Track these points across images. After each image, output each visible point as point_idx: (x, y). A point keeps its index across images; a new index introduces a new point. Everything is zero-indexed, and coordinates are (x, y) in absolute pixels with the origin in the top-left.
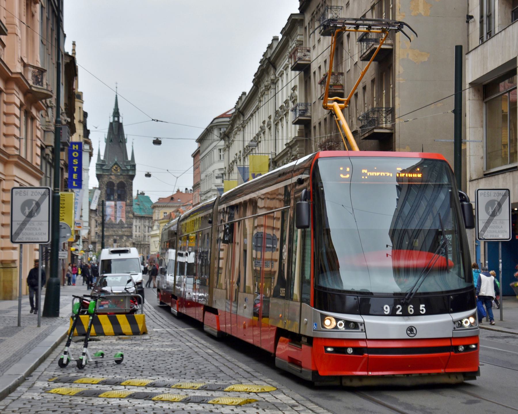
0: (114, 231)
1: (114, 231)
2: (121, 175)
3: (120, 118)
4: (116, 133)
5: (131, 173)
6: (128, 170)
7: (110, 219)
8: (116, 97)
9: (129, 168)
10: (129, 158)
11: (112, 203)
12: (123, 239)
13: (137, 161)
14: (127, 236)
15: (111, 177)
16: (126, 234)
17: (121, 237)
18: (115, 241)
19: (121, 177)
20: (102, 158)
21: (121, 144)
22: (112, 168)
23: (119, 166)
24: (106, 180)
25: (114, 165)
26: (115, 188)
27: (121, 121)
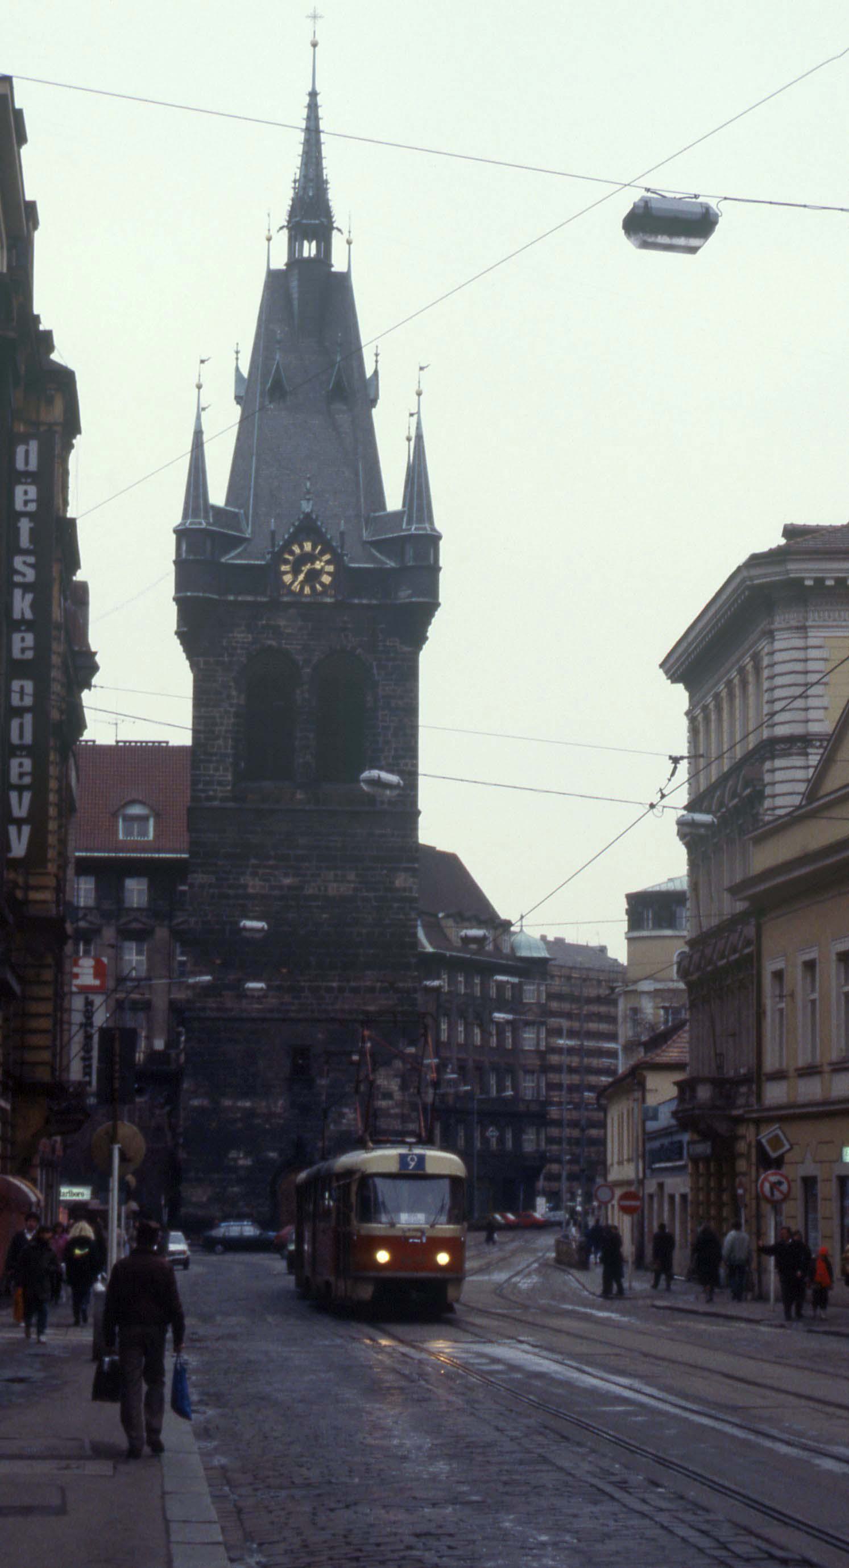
3: (337, 241)
4: (308, 342)
8: (313, 107)
13: (442, 519)
20: (217, 495)
21: (338, 406)
22: (278, 558)
25: (296, 537)
27: (338, 264)
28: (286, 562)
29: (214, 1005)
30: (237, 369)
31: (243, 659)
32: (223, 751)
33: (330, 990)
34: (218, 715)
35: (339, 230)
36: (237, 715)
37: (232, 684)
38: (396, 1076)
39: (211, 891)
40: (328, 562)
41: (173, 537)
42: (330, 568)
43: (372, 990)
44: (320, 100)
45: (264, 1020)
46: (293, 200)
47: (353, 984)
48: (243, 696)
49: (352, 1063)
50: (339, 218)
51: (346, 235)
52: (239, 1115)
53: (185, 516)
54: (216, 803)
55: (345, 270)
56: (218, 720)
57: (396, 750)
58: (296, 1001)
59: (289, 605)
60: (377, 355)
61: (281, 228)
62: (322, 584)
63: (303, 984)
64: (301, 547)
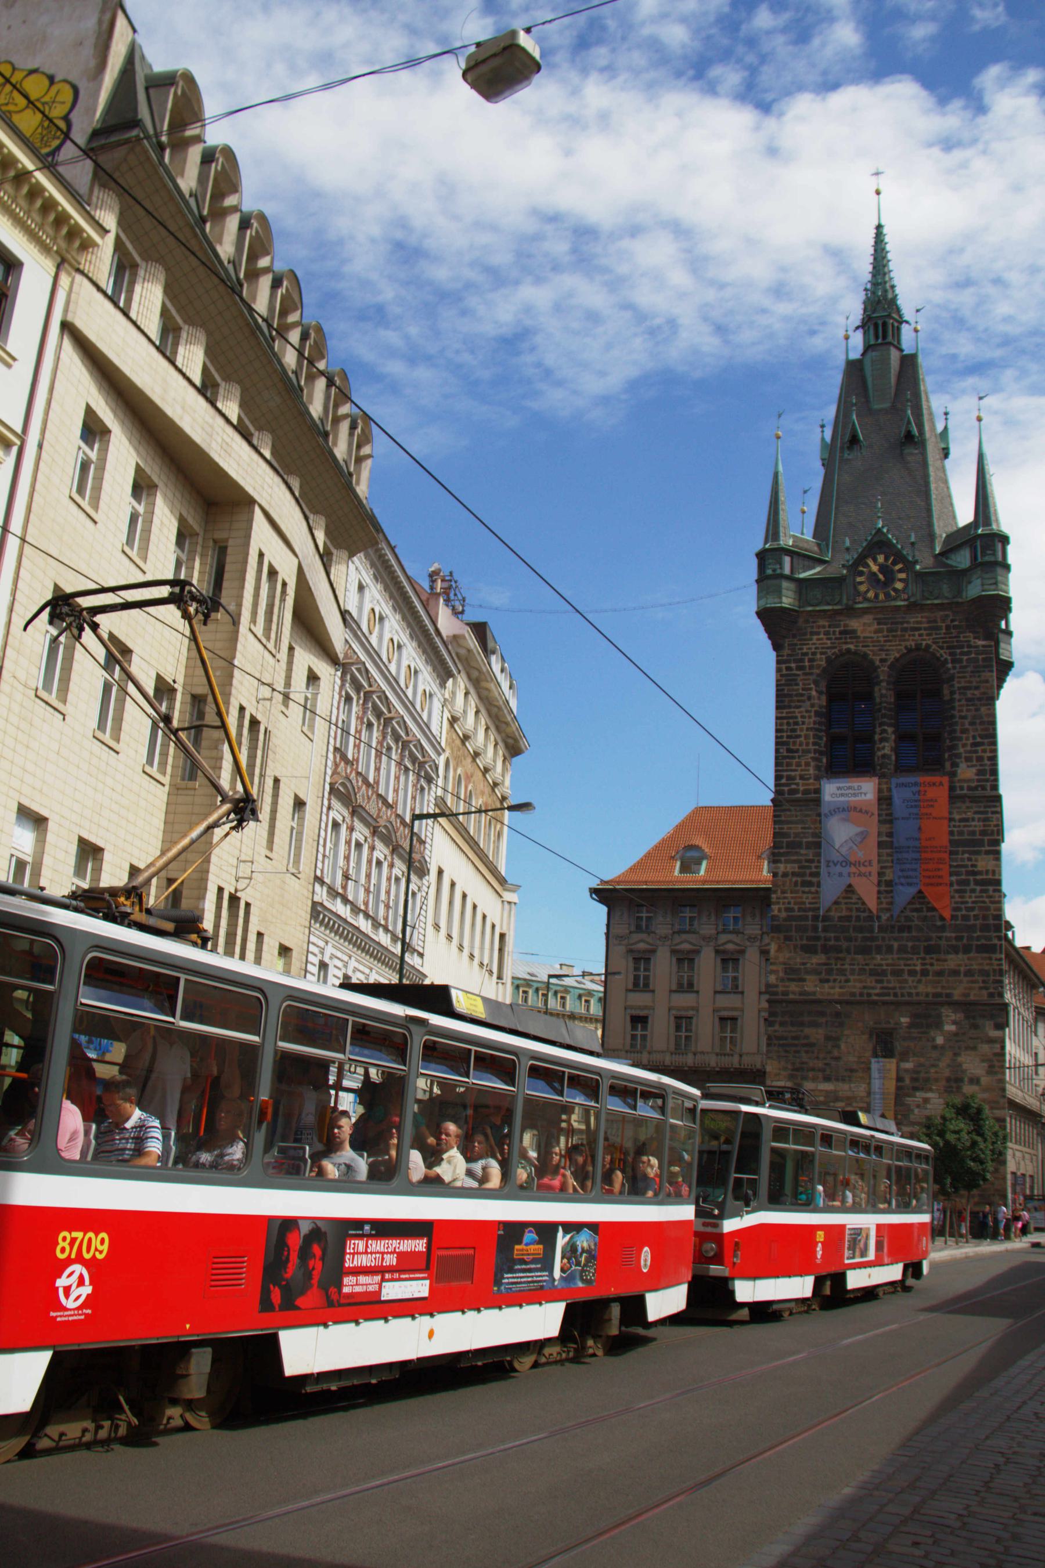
0: (878, 973)
1: (878, 973)
2: (913, 607)
3: (906, 331)
5: (974, 590)
6: (960, 576)
7: (850, 889)
9: (962, 560)
10: (964, 514)
11: (865, 790)
12: (938, 1025)
14: (966, 1006)
15: (854, 624)
16: (957, 994)
17: (926, 1015)
18: (885, 1044)
19: (913, 619)
23: (899, 557)
24: (820, 645)
26: (884, 693)
28: (861, 574)
29: (797, 989)
30: (823, 439)
31: (823, 663)
32: (804, 747)
33: (912, 973)
34: (799, 715)
35: (907, 322)
36: (817, 713)
37: (812, 686)
38: (983, 1061)
39: (794, 879)
40: (900, 571)
41: (755, 562)
42: (903, 576)
43: (955, 973)
44: (885, 231)
45: (848, 1003)
46: (864, 303)
47: (936, 968)
48: (824, 697)
49: (935, 1047)
50: (907, 313)
51: (913, 325)
52: (822, 1099)
53: (766, 542)
54: (800, 795)
55: (913, 352)
56: (800, 719)
57: (974, 737)
58: (879, 985)
59: (865, 611)
60: (946, 414)
61: (857, 328)
62: (895, 590)
63: (885, 967)
64: (875, 560)
